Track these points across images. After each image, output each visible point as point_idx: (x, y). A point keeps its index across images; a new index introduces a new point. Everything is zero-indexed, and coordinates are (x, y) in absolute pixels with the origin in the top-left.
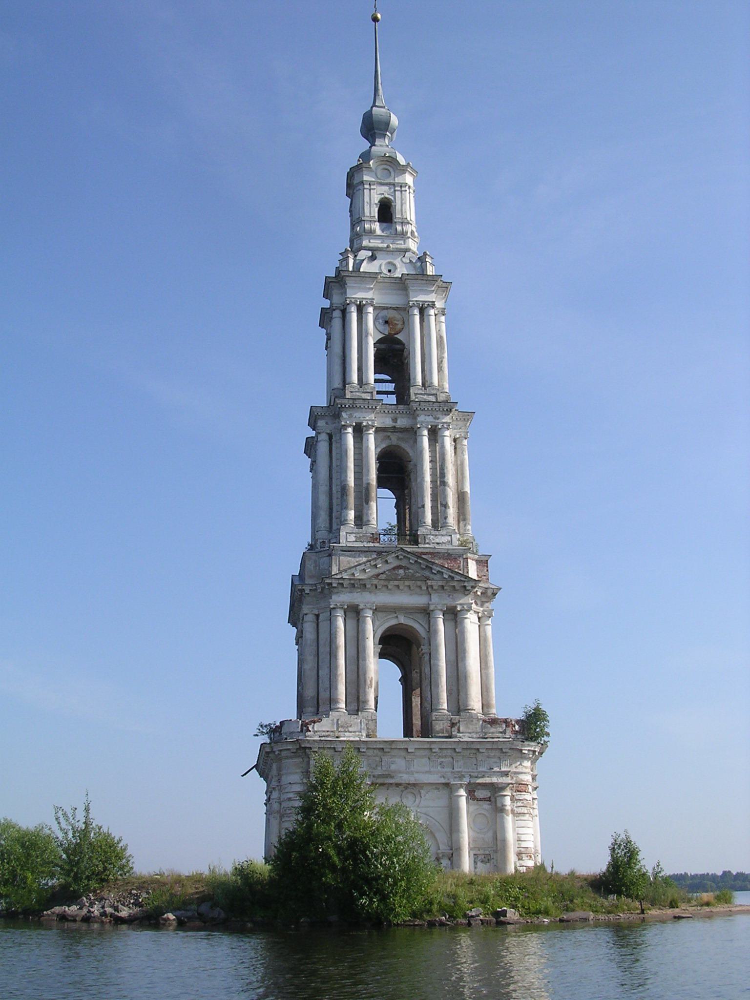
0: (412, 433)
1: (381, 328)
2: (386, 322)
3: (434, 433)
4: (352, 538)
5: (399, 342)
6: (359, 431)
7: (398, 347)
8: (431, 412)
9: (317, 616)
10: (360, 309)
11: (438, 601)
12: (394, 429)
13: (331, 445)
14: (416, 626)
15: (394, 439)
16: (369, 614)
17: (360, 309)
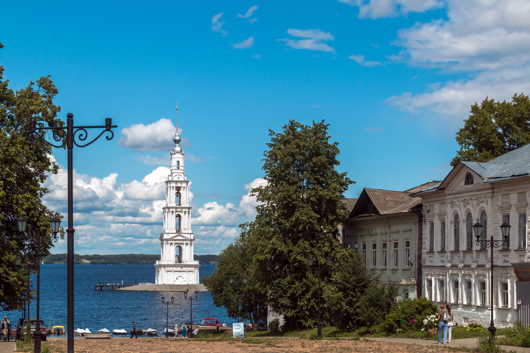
3: (185, 212)
6: (173, 212)
10: (173, 187)
17: (173, 187)
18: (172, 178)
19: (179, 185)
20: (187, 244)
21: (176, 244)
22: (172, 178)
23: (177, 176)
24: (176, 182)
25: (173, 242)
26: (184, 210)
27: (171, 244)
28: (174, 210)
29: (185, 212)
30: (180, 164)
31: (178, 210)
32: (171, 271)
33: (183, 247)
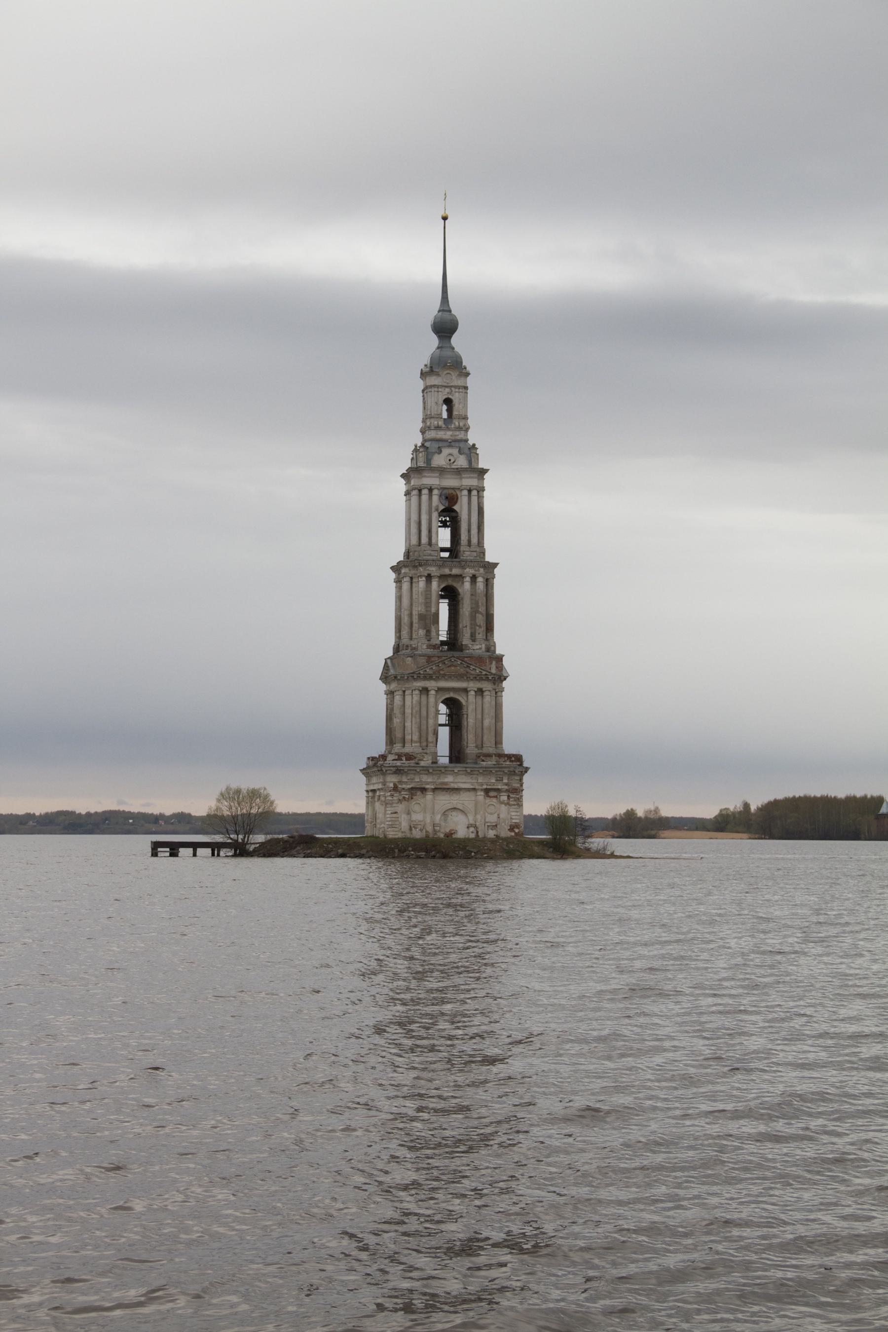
0: (460, 577)
1: (444, 502)
2: (447, 498)
4: (425, 647)
5: (454, 511)
6: (429, 578)
7: (454, 514)
8: (473, 567)
9: (404, 692)
10: (431, 490)
11: (472, 685)
12: (450, 575)
13: (412, 583)
14: (460, 698)
15: (450, 582)
16: (433, 692)
17: (431, 490)
18: (428, 461)
19: (450, 482)
20: (480, 692)
21: (440, 690)
22: (428, 461)
23: (446, 451)
24: (441, 471)
25: (431, 684)
26: (469, 571)
27: (425, 691)
28: (433, 570)
29: (474, 578)
30: (455, 413)
31: (447, 571)
32: (423, 790)
33: (470, 703)
